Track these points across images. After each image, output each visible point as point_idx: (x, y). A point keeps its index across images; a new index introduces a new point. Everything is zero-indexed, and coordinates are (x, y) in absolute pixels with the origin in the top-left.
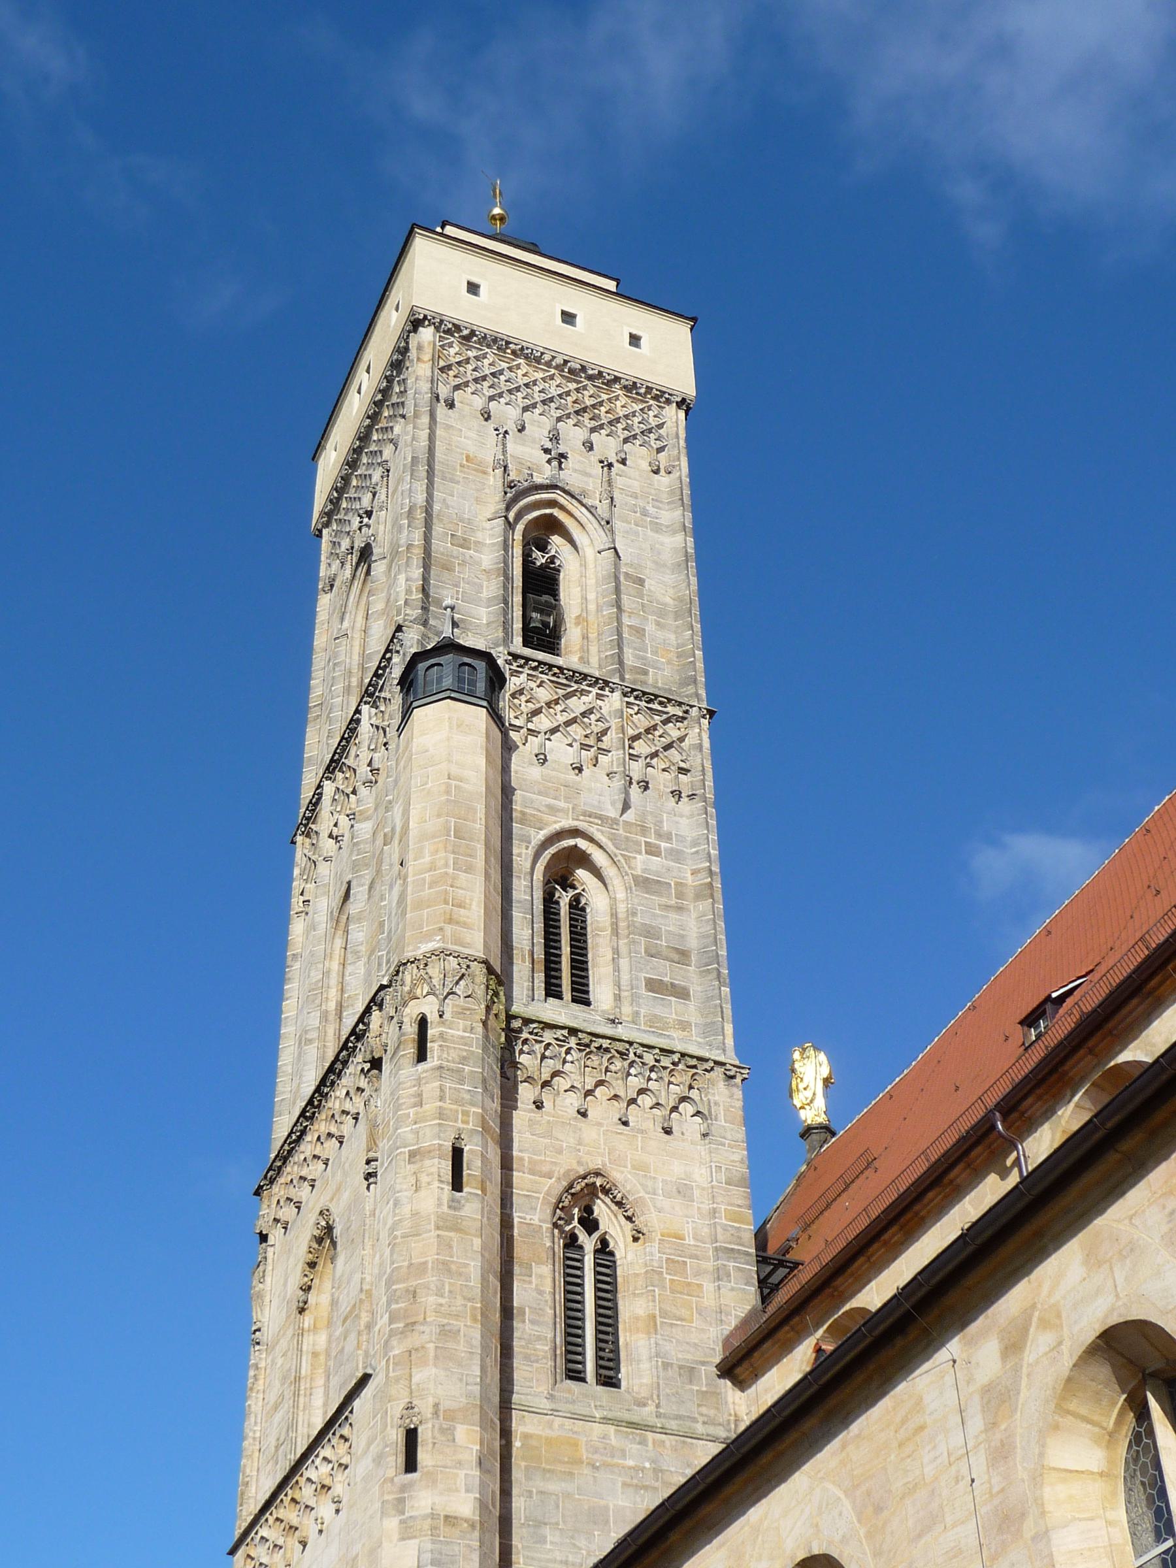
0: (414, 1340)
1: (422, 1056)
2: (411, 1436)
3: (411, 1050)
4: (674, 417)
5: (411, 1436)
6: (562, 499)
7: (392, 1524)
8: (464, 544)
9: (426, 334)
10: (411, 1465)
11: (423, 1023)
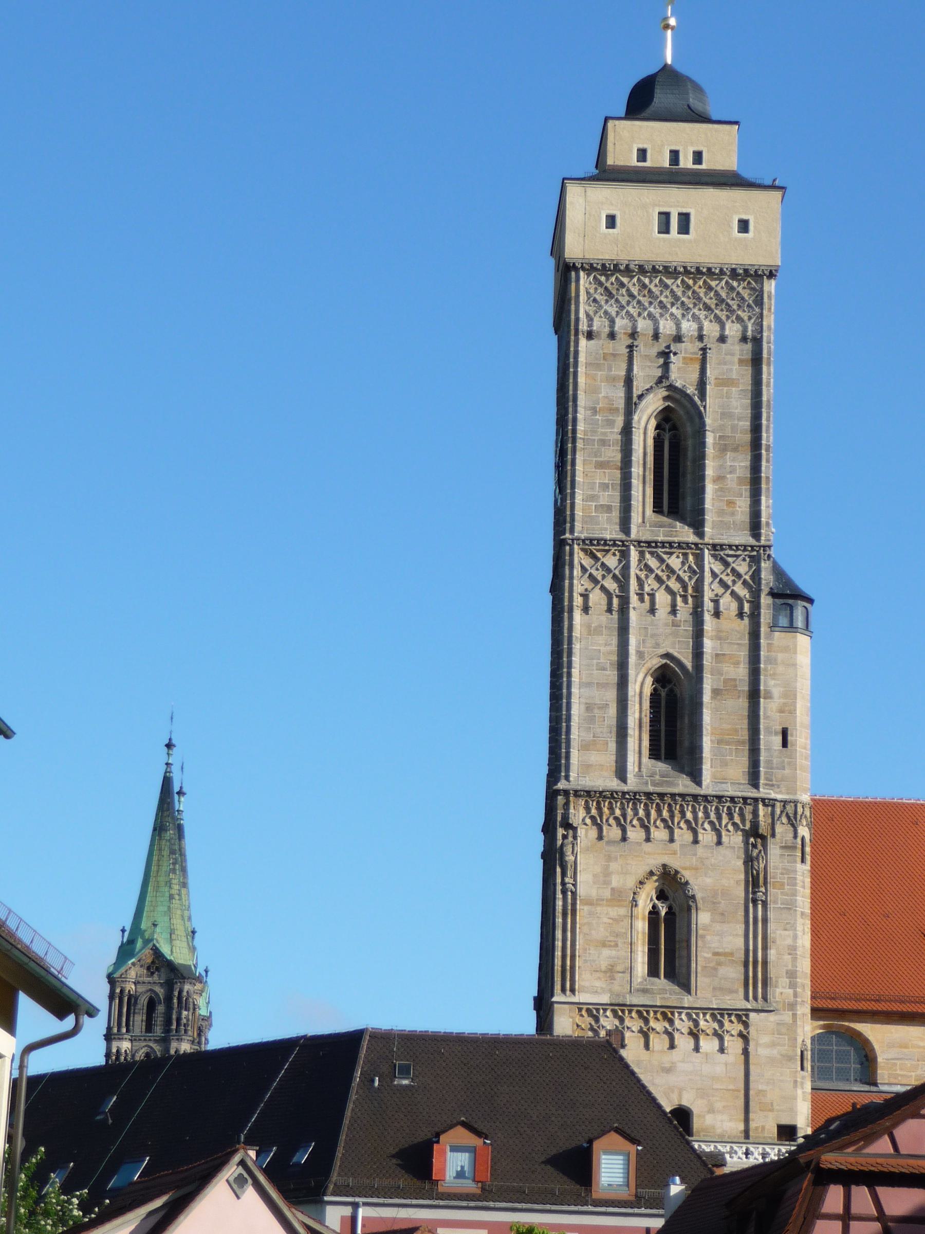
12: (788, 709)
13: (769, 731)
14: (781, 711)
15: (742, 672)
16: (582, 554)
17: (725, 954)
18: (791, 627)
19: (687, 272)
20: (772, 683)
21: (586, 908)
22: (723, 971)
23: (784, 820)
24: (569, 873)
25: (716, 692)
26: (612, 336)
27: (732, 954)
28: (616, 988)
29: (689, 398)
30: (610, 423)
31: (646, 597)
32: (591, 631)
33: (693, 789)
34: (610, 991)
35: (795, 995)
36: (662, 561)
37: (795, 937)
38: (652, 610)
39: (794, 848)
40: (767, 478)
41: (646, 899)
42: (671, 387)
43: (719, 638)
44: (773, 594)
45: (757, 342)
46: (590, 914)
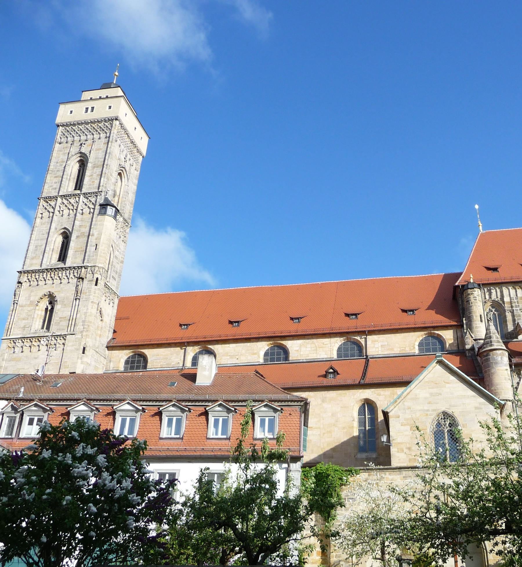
0: (87, 333)
1: (96, 285)
2: (84, 348)
3: (95, 283)
4: (141, 159)
5: (84, 348)
6: (124, 171)
7: (79, 361)
8: (111, 175)
9: (117, 122)
10: (83, 353)
11: (97, 279)
12: (98, 239)
13: (91, 246)
14: (96, 239)
15: (87, 229)
16: (44, 202)
17: (64, 318)
18: (105, 213)
19: (91, 122)
20: (95, 231)
21: (20, 308)
22: (61, 323)
23: (91, 272)
24: (17, 297)
25: (77, 237)
26: (67, 143)
27: (65, 317)
28: (25, 333)
29: (87, 156)
30: (61, 165)
31: (61, 212)
32: (42, 224)
33: (64, 266)
34: (23, 334)
35: (84, 328)
36: (68, 200)
37: (87, 309)
38: (62, 216)
39: (92, 281)
40: (105, 173)
41: (45, 303)
42: (81, 153)
43: (82, 221)
44: (100, 205)
45: (109, 137)
46: (22, 310)
